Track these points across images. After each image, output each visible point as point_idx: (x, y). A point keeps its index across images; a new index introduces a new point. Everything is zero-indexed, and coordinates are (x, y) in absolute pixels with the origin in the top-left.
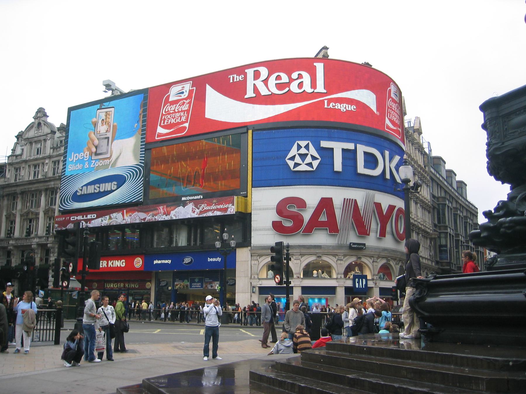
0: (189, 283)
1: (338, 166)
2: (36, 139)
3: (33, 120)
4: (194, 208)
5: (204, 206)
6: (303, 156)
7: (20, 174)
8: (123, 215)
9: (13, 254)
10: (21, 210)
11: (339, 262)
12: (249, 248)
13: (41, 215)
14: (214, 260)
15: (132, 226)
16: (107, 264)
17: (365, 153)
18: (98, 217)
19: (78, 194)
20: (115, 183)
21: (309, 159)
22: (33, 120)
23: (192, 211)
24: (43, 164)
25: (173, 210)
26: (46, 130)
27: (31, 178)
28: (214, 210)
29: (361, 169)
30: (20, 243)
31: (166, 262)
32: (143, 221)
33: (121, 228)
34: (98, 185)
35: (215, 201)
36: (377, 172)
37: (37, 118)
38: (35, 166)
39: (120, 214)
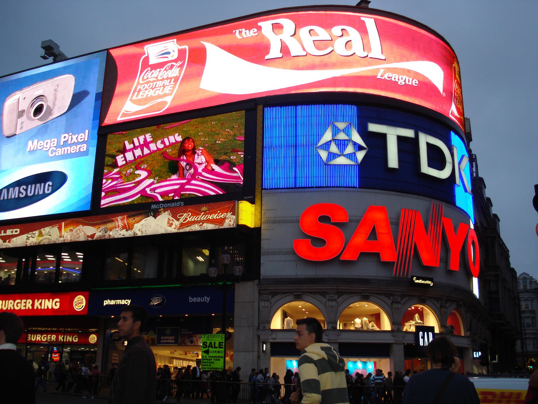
0: (155, 337)
1: (393, 161)
4: (171, 218)
5: (187, 217)
6: (342, 145)
8: (60, 229)
11: (395, 305)
12: (257, 282)
14: (199, 300)
15: (72, 247)
16: (33, 305)
17: (429, 145)
18: (21, 233)
21: (350, 149)
23: (168, 223)
25: (138, 222)
28: (203, 222)
31: (123, 302)
32: (90, 239)
33: (56, 249)
34: (25, 187)
35: (204, 209)
39: (56, 229)
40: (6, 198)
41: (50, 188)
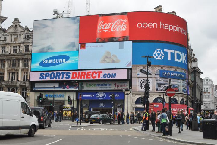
2: (14, 33)
3: (12, 24)
7: (5, 50)
9: (4, 89)
10: (7, 68)
13: (20, 71)
19: (44, 63)
20: (65, 59)
22: (12, 24)
24: (19, 46)
26: (19, 29)
27: (12, 53)
29: (176, 60)
30: (7, 84)
31: (90, 96)
36: (180, 61)
37: (15, 23)
38: (14, 47)
40: (48, 63)
41: (65, 61)
